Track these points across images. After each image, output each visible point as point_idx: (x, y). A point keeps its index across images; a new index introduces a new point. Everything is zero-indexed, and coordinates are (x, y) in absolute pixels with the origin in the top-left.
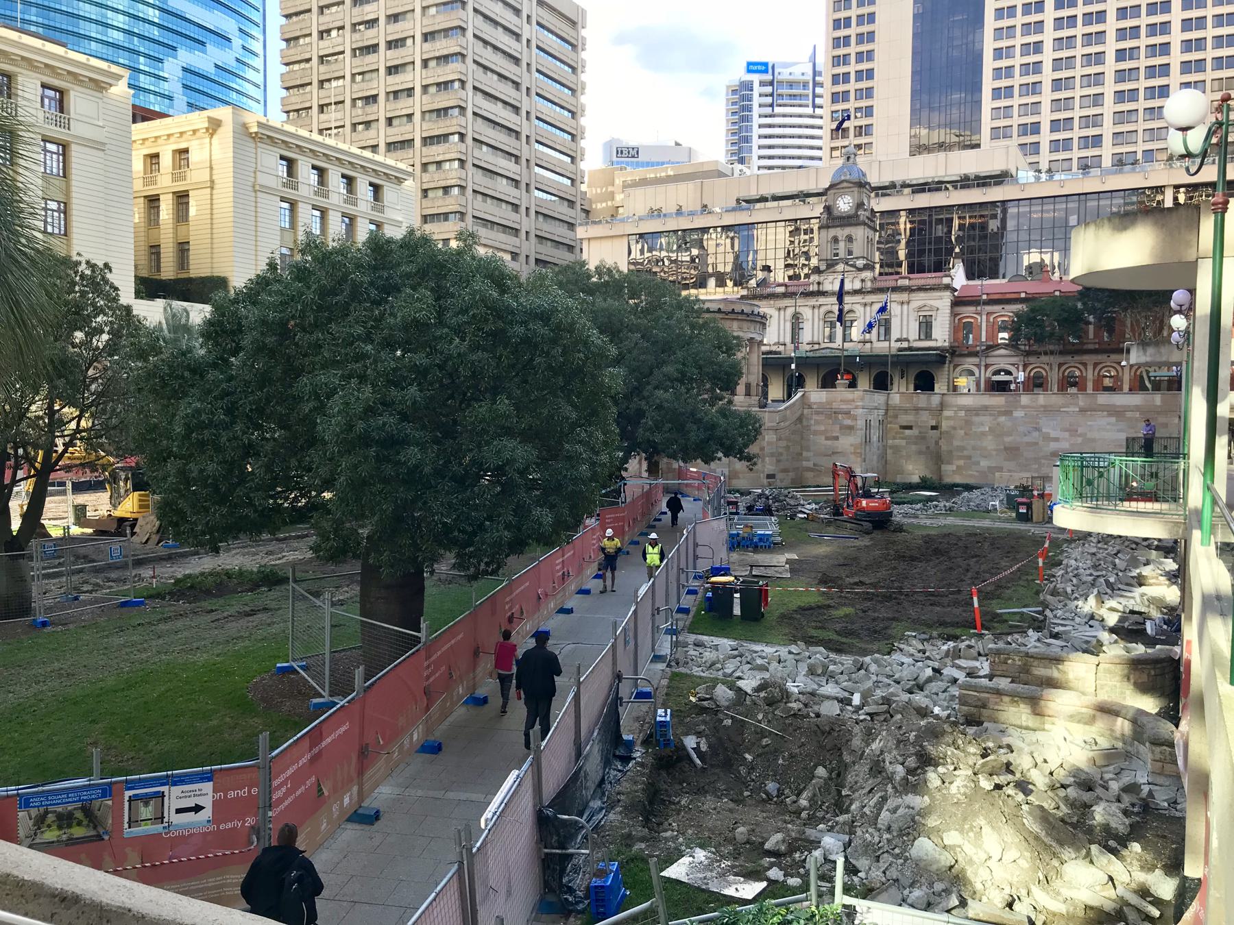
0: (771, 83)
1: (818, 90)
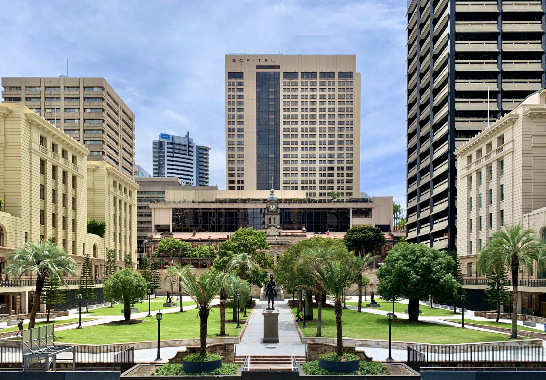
1: (190, 149)
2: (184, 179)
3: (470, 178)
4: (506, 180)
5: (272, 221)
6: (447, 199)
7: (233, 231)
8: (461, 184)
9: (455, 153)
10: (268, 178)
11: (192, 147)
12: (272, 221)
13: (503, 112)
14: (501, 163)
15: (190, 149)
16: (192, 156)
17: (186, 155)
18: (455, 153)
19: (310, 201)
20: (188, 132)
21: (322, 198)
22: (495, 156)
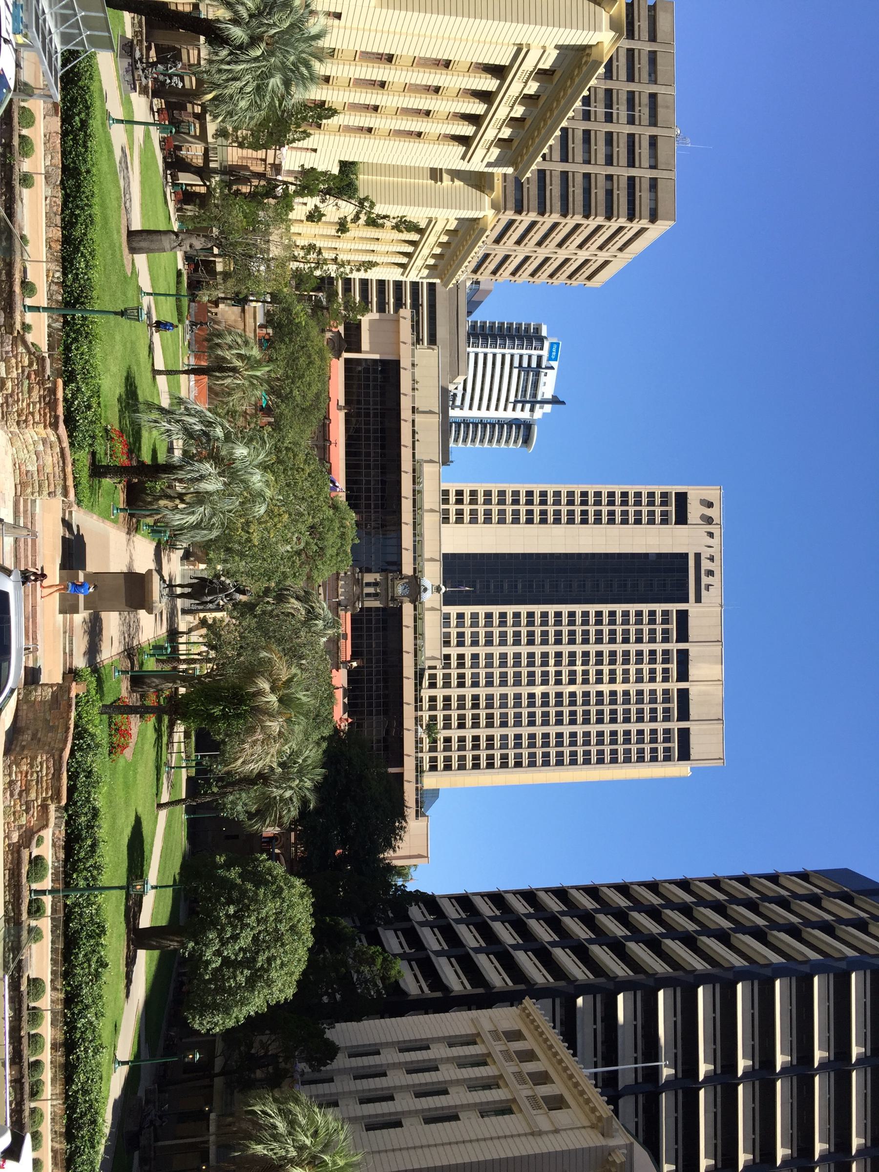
0: (539, 365)
1: (528, 406)
2: (465, 389)
3: (470, 1040)
4: (471, 1125)
5: (371, 590)
6: (426, 989)
7: (348, 498)
8: (458, 1022)
9: (527, 1002)
10: (475, 578)
11: (532, 410)
12: (371, 590)
13: (613, 1101)
14: (505, 1109)
15: (528, 406)
16: (514, 410)
17: (516, 396)
18: (527, 1002)
19: (419, 675)
20: (563, 403)
21: (426, 704)
22: (524, 1092)
